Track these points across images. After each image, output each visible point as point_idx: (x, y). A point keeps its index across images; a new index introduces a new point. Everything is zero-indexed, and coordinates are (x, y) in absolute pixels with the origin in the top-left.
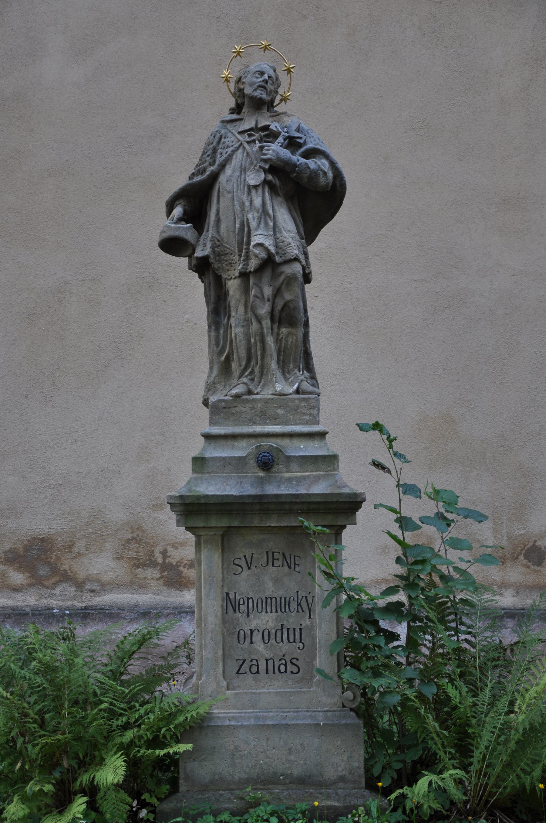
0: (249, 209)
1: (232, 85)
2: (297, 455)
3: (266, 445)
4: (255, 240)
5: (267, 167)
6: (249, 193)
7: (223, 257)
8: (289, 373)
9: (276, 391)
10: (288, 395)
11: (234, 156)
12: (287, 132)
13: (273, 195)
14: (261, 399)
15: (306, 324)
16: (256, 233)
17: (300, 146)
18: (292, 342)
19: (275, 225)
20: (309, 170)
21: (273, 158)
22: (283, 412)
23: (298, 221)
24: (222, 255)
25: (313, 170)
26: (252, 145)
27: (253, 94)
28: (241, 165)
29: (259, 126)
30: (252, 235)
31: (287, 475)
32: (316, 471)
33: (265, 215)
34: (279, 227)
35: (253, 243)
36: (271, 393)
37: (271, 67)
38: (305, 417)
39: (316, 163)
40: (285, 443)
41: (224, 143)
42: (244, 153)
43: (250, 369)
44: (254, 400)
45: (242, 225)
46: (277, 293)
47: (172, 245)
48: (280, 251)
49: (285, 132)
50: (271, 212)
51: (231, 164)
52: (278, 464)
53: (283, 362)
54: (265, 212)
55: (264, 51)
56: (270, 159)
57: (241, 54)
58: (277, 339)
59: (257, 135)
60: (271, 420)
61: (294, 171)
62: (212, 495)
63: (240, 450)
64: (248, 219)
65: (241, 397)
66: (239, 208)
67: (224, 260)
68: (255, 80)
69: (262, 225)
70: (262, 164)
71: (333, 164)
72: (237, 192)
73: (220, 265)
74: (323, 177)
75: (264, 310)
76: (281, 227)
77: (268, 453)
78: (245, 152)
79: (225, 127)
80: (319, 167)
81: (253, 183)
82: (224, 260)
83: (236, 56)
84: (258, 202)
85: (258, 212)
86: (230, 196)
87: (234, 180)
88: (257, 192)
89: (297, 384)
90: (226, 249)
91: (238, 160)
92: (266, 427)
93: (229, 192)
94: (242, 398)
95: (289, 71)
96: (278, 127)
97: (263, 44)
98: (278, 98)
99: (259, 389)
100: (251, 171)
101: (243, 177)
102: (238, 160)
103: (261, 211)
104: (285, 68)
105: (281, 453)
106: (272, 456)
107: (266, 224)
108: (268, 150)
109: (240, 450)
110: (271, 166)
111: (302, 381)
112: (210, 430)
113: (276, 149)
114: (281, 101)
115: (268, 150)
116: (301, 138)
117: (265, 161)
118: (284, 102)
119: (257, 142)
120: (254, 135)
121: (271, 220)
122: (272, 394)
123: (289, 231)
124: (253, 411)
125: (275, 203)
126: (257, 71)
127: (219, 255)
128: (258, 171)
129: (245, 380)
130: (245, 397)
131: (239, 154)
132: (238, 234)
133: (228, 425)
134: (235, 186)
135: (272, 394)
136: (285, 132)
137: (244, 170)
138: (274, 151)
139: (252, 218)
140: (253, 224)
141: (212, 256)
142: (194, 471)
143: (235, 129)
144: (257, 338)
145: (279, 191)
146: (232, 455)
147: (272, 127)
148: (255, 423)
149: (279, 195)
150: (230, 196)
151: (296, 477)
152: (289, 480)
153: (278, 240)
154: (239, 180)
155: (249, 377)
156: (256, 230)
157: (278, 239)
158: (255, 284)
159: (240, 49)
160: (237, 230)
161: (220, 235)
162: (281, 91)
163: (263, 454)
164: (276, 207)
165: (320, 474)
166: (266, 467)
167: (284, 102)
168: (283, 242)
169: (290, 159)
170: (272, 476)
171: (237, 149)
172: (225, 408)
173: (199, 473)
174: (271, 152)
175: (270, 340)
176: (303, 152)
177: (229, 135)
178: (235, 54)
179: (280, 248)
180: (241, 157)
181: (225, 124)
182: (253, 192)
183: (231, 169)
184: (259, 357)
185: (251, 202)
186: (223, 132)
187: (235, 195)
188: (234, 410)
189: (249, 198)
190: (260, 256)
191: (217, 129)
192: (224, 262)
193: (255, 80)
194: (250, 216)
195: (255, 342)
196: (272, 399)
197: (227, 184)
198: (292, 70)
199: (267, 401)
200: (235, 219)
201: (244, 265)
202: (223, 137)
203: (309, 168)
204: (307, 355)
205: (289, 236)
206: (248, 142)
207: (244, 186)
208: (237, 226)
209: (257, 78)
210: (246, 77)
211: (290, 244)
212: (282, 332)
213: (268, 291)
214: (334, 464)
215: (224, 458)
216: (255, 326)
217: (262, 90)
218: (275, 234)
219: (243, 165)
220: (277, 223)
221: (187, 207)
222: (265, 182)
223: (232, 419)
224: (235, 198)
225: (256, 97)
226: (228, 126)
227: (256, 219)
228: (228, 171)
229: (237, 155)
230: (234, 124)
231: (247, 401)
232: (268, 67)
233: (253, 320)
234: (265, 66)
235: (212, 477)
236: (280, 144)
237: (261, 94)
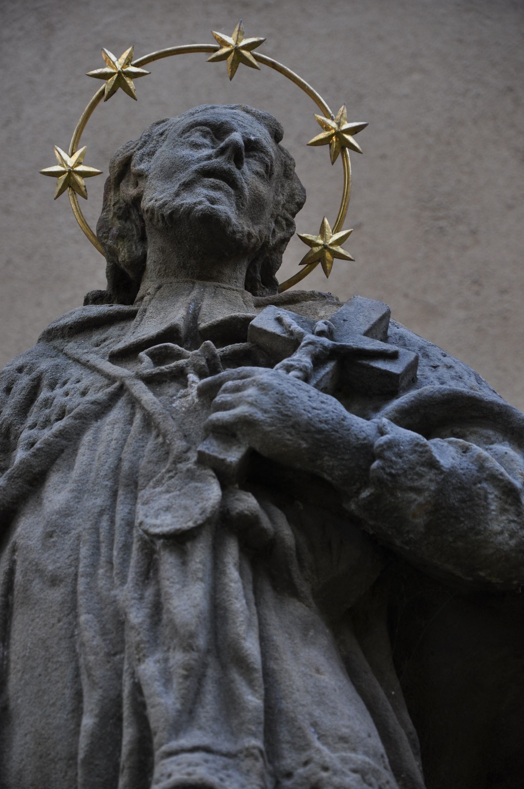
0: (143, 636)
5: (233, 456)
6: (149, 571)
11: (87, 438)
12: (329, 334)
13: (269, 595)
16: (174, 744)
19: (273, 716)
20: (431, 474)
21: (259, 416)
23: (393, 720)
25: (452, 473)
26: (171, 389)
27: (178, 201)
28: (117, 467)
29: (202, 325)
30: (157, 754)
33: (224, 667)
41: (47, 403)
42: (130, 422)
45: (110, 717)
49: (321, 333)
50: (251, 646)
51: (71, 468)
54: (222, 650)
56: (247, 423)
57: (131, 83)
59: (192, 356)
61: (363, 478)
64: (137, 688)
66: (97, 641)
68: (186, 152)
70: (212, 448)
72: (92, 575)
74: (503, 511)
78: (138, 416)
80: (482, 468)
81: (165, 523)
83: (113, 91)
84: (186, 600)
85: (188, 648)
86: (57, 595)
87: (81, 525)
88: (184, 563)
91: (101, 449)
93: (54, 581)
95: (338, 144)
97: (223, 43)
100: (159, 483)
101: (121, 511)
102: (101, 449)
103: (201, 642)
107: (230, 703)
108: (237, 389)
110: (252, 455)
114: (310, 262)
115: (237, 389)
116: (393, 356)
117: (225, 433)
119: (192, 377)
120: (180, 356)
121: (251, 683)
123: (343, 739)
125: (273, 619)
128: (191, 476)
134: (84, 551)
136: (321, 333)
139: (159, 679)
140: (164, 703)
145: (295, 568)
149: (295, 594)
150: (57, 595)
154: (104, 524)
156: (177, 728)
157: (289, 775)
159: (128, 62)
160: (83, 742)
162: (304, 224)
164: (279, 638)
171: (103, 409)
177: (75, 371)
178: (107, 85)
180: (116, 434)
181: (57, 343)
182: (168, 563)
185: (157, 609)
186: (44, 365)
187: (81, 588)
189: (149, 593)
191: (19, 362)
193: (186, 152)
194: (149, 668)
197: (45, 547)
200: (79, 695)
202: (45, 382)
206: (151, 381)
207: (126, 547)
208: (88, 721)
209: (196, 146)
210: (151, 154)
218: (271, 751)
219: (126, 466)
220: (286, 705)
222: (223, 524)
224: (81, 600)
225: (190, 210)
226: (72, 347)
227: (176, 681)
228: (56, 494)
229: (98, 430)
230: (96, 337)
237: (213, 201)
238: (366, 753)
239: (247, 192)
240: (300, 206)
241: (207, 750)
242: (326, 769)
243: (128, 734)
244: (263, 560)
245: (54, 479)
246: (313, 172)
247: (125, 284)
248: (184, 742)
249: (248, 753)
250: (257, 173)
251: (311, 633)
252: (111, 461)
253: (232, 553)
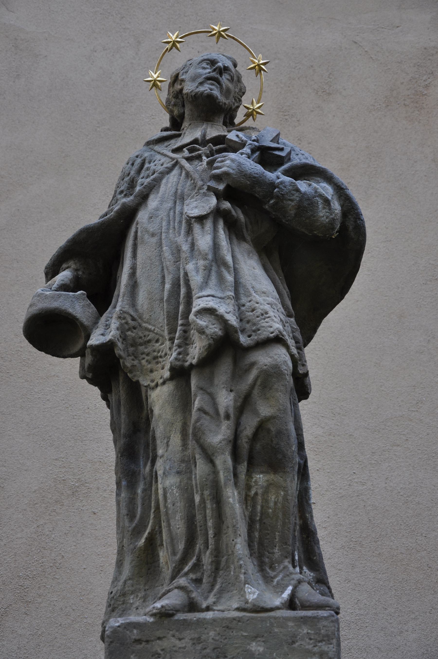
0: (188, 255)
4: (199, 304)
5: (221, 187)
6: (189, 231)
7: (141, 348)
8: (272, 567)
9: (247, 602)
11: (164, 181)
12: (257, 141)
13: (235, 241)
14: (214, 620)
15: (303, 473)
16: (201, 294)
18: (276, 503)
19: (237, 285)
20: (297, 194)
21: (231, 171)
23: (281, 287)
24: (141, 344)
25: (305, 194)
26: (196, 162)
27: (198, 90)
28: (176, 192)
29: (207, 138)
30: (194, 298)
33: (219, 267)
34: (244, 286)
35: (194, 310)
36: (236, 605)
41: (148, 169)
42: (181, 175)
44: (200, 623)
45: (176, 285)
46: (245, 404)
47: (49, 331)
48: (248, 326)
49: (254, 141)
50: (229, 258)
51: (158, 193)
53: (261, 544)
54: (217, 260)
56: (226, 174)
57: (178, 45)
58: (247, 496)
59: (203, 150)
61: (271, 195)
64: (186, 274)
65: (172, 615)
66: (170, 257)
68: (200, 71)
70: (213, 184)
71: (340, 190)
72: (167, 233)
73: (136, 362)
74: (324, 208)
75: (218, 436)
78: (184, 173)
80: (316, 192)
81: (196, 212)
82: (142, 354)
83: (171, 48)
84: (204, 241)
85: (205, 259)
86: (154, 240)
87: (163, 214)
88: (203, 228)
89: (290, 588)
90: (147, 333)
91: (169, 185)
93: (153, 235)
94: (176, 618)
95: (259, 69)
97: (214, 29)
99: (211, 599)
100: (192, 198)
101: (178, 208)
102: (169, 185)
103: (210, 257)
107: (221, 280)
108: (222, 161)
110: (228, 187)
111: (300, 582)
115: (222, 161)
116: (282, 149)
117: (218, 178)
119: (204, 158)
120: (199, 150)
121: (229, 272)
122: (238, 609)
124: (199, 647)
125: (236, 249)
127: (134, 344)
128: (205, 195)
129: (182, 581)
130: (180, 616)
132: (168, 300)
134: (164, 224)
135: (238, 609)
139: (194, 270)
140: (196, 279)
141: (119, 344)
144: (207, 493)
145: (245, 231)
149: (245, 240)
150: (154, 240)
153: (243, 308)
154: (172, 213)
155: (192, 576)
156: (201, 288)
157: (244, 305)
158: (202, 389)
159: (177, 37)
160: (166, 294)
161: (136, 311)
162: (245, 101)
164: (239, 256)
168: (253, 310)
171: (170, 170)
175: (232, 497)
177: (158, 157)
178: (169, 46)
179: (248, 322)
180: (175, 179)
181: (151, 146)
182: (197, 228)
184: (211, 533)
185: (193, 245)
186: (146, 154)
187: (163, 237)
189: (190, 239)
190: (208, 331)
191: (137, 154)
192: (144, 356)
193: (200, 71)
194: (190, 267)
195: (203, 501)
196: (239, 620)
197: (149, 222)
199: (228, 625)
200: (163, 277)
201: (179, 354)
202: (147, 161)
204: (308, 535)
205: (264, 300)
206: (188, 159)
207: (180, 222)
208: (167, 286)
209: (204, 68)
210: (186, 72)
211: (267, 313)
212: (256, 482)
213: (226, 400)
216: (201, 468)
217: (212, 84)
218: (237, 297)
219: (179, 191)
220: (242, 280)
221: (80, 273)
222: (217, 213)
224: (164, 242)
225: (202, 93)
226: (157, 148)
227: (201, 271)
228: (153, 202)
229: (168, 178)
230: (166, 144)
231: (186, 624)
233: (197, 456)
237: (211, 90)
238: (272, 298)
239: (224, 86)
240: (244, 93)
241: (213, 296)
242: (258, 303)
243: (183, 290)
244: (232, 227)
245: (152, 197)
246: (249, 81)
247: (176, 124)
248: (204, 293)
249: (229, 298)
250: (228, 79)
251: (251, 255)
252: (173, 190)
253: (221, 225)
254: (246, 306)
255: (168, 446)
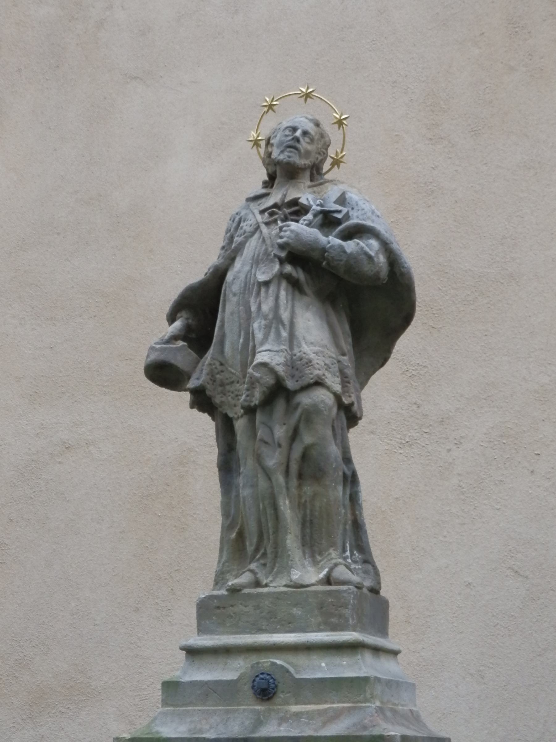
1: (262, 151)
2: (312, 677)
3: (267, 662)
4: (260, 358)
5: (283, 254)
7: (228, 387)
8: (320, 554)
9: (291, 581)
10: (308, 586)
11: (247, 245)
12: (321, 205)
14: (269, 594)
15: (351, 480)
17: (338, 222)
18: (320, 507)
21: (290, 241)
22: (300, 613)
24: (228, 384)
25: (351, 254)
26: (272, 226)
28: (254, 256)
29: (286, 201)
31: (295, 708)
32: (339, 702)
34: (298, 338)
35: (255, 363)
36: (284, 583)
37: (311, 120)
38: (333, 620)
39: (358, 244)
40: (301, 660)
43: (262, 551)
44: (259, 595)
46: (295, 435)
47: (163, 374)
48: (297, 373)
49: (318, 205)
51: (242, 255)
52: (283, 692)
53: (311, 537)
55: (306, 100)
58: (299, 503)
60: (283, 625)
62: (176, 738)
63: (230, 671)
65: (239, 590)
67: (229, 392)
69: (272, 335)
71: (386, 246)
73: (224, 399)
74: (369, 264)
75: (273, 460)
76: (301, 338)
77: (268, 675)
79: (248, 207)
82: (229, 392)
83: (268, 111)
85: (266, 319)
89: (327, 570)
90: (231, 375)
91: (250, 249)
92: (274, 635)
94: (243, 592)
95: (340, 123)
96: (310, 199)
97: (302, 92)
98: (329, 161)
99: (270, 579)
102: (250, 249)
103: (271, 316)
104: (335, 121)
105: (287, 674)
106: (274, 680)
107: (278, 334)
109: (230, 671)
110: (290, 253)
111: (336, 565)
112: (195, 640)
113: (302, 229)
114: (333, 165)
116: (339, 212)
118: (336, 166)
120: (277, 214)
121: (284, 328)
122: (286, 586)
123: (312, 343)
124: (258, 611)
126: (287, 128)
127: (222, 385)
129: (253, 566)
130: (246, 591)
131: (253, 242)
133: (222, 633)
135: (286, 586)
136: (318, 205)
137: (256, 262)
138: (292, 231)
140: (259, 336)
141: (208, 386)
142: (165, 703)
143: (256, 208)
144: (266, 502)
146: (219, 679)
147: (303, 201)
148: (260, 630)
151: (308, 712)
152: (298, 715)
153: (294, 358)
155: (262, 561)
156: (262, 344)
158: (263, 423)
159: (272, 101)
161: (224, 357)
162: (331, 152)
163: (261, 676)
165: (344, 707)
166: (265, 696)
167: (336, 166)
168: (301, 360)
169: (316, 241)
170: (274, 710)
171: (253, 234)
172: (218, 608)
173: (171, 705)
174: (288, 233)
175: (285, 506)
176: (341, 231)
178: (266, 109)
179: (297, 369)
180: (255, 244)
182: (263, 290)
183: (241, 262)
184: (271, 531)
188: (230, 610)
189: (258, 300)
190: (262, 382)
191: (237, 211)
192: (230, 394)
195: (264, 509)
196: (285, 593)
198: (345, 122)
199: (278, 597)
201: (247, 396)
202: (242, 220)
203: (345, 252)
204: (357, 527)
205: (311, 350)
206: (267, 224)
208: (241, 340)
210: (276, 136)
211: (310, 362)
212: (305, 493)
213: (280, 432)
214: (365, 691)
215: (207, 683)
216: (263, 483)
217: (291, 152)
219: (256, 255)
220: (297, 333)
221: (190, 321)
222: (282, 276)
223: (228, 625)
227: (262, 329)
228: (238, 264)
229: (250, 242)
230: (259, 202)
231: (249, 595)
232: (306, 121)
233: (259, 476)
234: (302, 119)
235: (188, 711)
236: (306, 222)
237: (289, 157)
238: (319, 347)
239: (302, 151)
240: (329, 146)
241: (269, 350)
242: (304, 353)
243: (251, 344)
244: (295, 285)
245: (238, 259)
247: (270, 182)
248: (263, 348)
249: (282, 351)
250: (308, 143)
251: (311, 307)
252: (252, 254)
253: (284, 284)
254: (297, 356)
255: (247, 466)
